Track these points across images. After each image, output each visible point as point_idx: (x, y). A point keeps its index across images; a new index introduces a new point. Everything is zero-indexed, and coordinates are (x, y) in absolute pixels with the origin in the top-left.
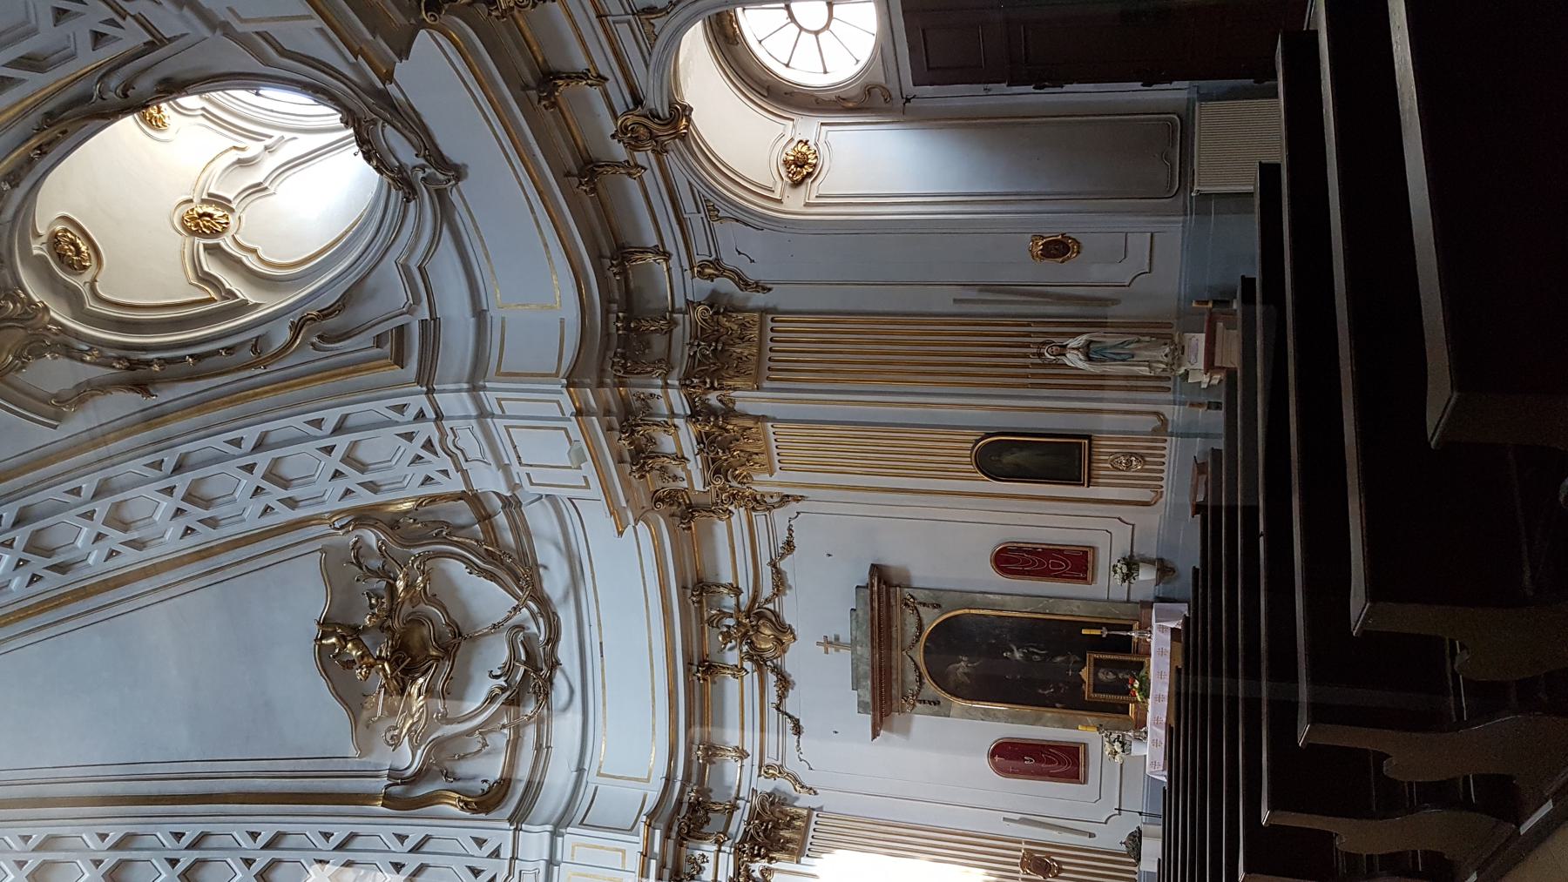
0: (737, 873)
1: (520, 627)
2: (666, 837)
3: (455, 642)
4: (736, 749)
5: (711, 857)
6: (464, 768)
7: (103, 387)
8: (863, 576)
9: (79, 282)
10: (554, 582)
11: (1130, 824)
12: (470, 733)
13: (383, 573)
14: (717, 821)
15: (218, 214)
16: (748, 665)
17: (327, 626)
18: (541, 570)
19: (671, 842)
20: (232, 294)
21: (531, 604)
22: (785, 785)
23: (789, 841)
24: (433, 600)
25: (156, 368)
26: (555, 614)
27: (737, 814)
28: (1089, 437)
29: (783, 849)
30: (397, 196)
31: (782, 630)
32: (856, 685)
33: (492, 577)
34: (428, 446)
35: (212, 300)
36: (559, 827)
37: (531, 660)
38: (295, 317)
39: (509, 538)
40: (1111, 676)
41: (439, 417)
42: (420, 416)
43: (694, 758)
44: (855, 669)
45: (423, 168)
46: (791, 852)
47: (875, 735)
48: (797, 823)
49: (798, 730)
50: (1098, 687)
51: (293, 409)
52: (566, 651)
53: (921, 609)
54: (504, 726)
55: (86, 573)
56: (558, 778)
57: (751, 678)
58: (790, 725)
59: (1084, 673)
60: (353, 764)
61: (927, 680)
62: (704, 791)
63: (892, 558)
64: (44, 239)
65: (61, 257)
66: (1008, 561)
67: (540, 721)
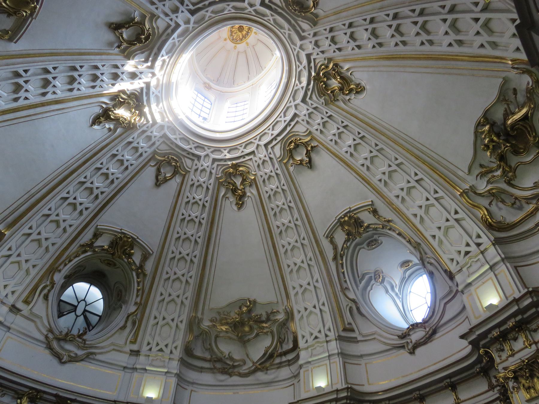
3: (243, 341)
6: (199, 343)
7: (335, 248)
9: (365, 245)
10: (261, 376)
12: (210, 344)
17: (254, 302)
18: (265, 372)
20: (360, 283)
21: (253, 368)
24: (257, 335)
25: (341, 262)
26: (249, 376)
30: (400, 333)
33: (264, 355)
34: (316, 338)
36: (179, 376)
37: (234, 367)
38: (357, 301)
39: (277, 361)
41: (327, 342)
42: (326, 336)
45: (411, 342)
51: (328, 297)
52: (235, 379)
54: (212, 356)
55: (278, 239)
56: (192, 375)
60: (206, 307)
65: (372, 241)
67: (211, 369)
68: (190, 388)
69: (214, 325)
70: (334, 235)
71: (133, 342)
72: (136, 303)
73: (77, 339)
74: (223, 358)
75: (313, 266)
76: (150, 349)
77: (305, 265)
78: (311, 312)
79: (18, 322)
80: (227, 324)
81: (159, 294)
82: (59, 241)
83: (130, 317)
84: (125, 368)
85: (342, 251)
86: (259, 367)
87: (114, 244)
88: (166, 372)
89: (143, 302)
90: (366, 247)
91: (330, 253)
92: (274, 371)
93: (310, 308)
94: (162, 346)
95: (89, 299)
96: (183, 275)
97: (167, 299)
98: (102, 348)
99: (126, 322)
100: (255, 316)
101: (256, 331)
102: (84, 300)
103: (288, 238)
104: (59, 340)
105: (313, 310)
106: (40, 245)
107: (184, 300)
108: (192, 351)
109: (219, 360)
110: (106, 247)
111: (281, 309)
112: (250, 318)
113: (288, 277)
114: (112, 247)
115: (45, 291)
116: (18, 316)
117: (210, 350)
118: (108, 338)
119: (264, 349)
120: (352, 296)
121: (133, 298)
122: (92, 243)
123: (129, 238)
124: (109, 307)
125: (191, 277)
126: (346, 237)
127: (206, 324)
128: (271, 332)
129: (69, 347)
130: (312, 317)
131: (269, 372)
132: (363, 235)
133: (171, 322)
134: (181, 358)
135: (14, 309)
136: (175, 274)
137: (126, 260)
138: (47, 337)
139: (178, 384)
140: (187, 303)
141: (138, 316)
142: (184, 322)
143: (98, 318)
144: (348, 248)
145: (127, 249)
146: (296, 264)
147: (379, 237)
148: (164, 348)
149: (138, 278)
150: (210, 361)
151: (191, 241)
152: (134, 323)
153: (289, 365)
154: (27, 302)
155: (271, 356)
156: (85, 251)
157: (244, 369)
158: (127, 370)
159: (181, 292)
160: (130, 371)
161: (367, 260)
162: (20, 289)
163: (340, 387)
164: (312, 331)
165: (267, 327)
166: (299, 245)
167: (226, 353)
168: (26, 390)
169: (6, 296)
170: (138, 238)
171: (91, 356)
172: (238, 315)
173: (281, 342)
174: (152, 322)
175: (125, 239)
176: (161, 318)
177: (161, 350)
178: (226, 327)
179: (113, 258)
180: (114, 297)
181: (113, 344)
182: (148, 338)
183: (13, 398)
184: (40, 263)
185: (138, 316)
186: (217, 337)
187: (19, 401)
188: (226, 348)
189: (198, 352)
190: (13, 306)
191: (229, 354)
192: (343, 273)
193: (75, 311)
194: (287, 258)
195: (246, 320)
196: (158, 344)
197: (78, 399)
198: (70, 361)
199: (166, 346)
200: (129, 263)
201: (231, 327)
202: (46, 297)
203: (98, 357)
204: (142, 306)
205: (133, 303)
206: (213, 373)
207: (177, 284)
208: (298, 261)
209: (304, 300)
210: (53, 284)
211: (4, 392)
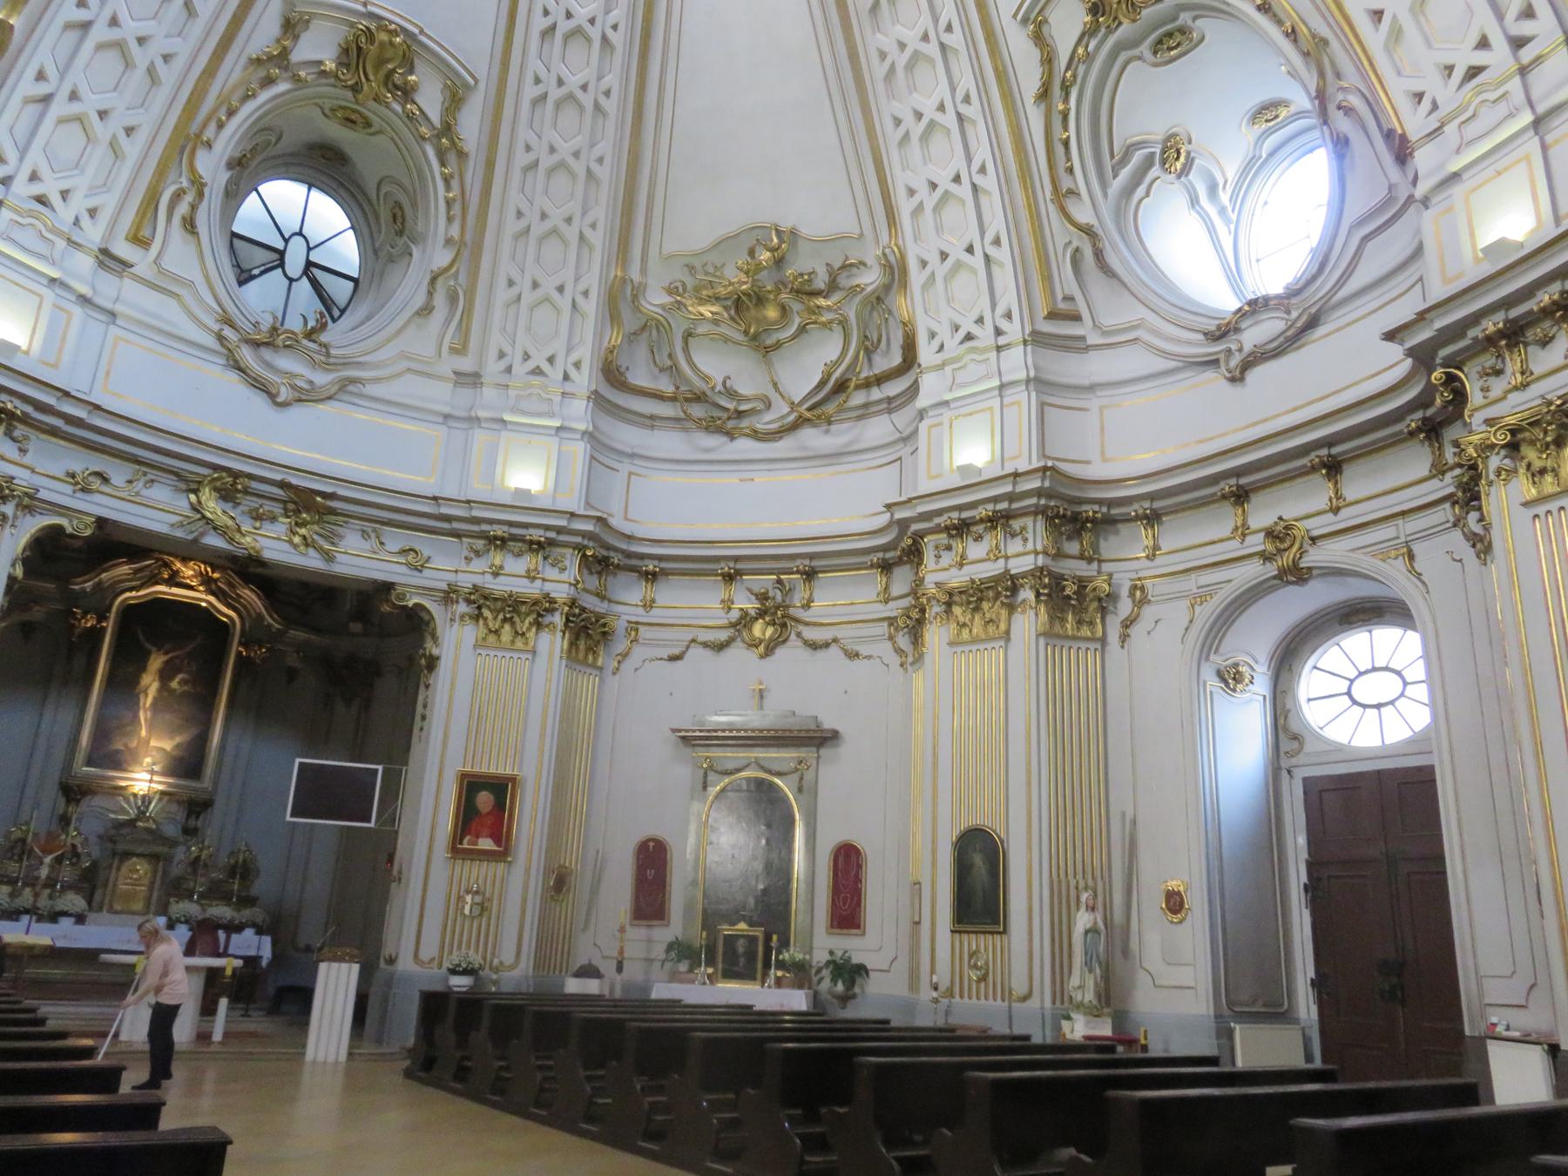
1: (769, 406)
2: (584, 534)
3: (763, 347)
6: (642, 352)
7: (1048, 60)
8: (828, 723)
9: (1145, 49)
10: (811, 437)
11: (607, 968)
12: (670, 356)
13: (833, 286)
14: (593, 582)
15: (1179, 165)
16: (735, 615)
17: (791, 236)
18: (825, 427)
19: (579, 540)
20: (1115, 177)
21: (792, 418)
22: (620, 645)
25: (1061, 107)
28: (1005, 932)
30: (1211, 326)
31: (770, 649)
33: (822, 383)
34: (969, 337)
35: (1112, 156)
36: (590, 437)
37: (740, 414)
38: (1100, 232)
40: (741, 950)
41: (999, 349)
42: (998, 332)
43: (646, 562)
45: (1240, 350)
46: (569, 651)
48: (590, 658)
49: (674, 658)
50: (730, 940)
51: (1013, 224)
52: (744, 447)
53: (796, 777)
55: (868, 31)
56: (627, 436)
58: (677, 651)
59: (742, 926)
63: (845, 750)
64: (1190, 23)
65: (1170, 35)
66: (847, 856)
68: (625, 467)
69: (679, 302)
70: (1047, 12)
71: (460, 350)
72: (449, 242)
73: (305, 342)
74: (709, 393)
75: (974, 122)
76: (509, 370)
77: (949, 119)
78: (959, 265)
79: (130, 295)
80: (717, 299)
81: (512, 213)
82: (183, 48)
83: (440, 280)
84: (447, 417)
85: (1068, 68)
86: (808, 415)
87: (354, 54)
88: (559, 429)
89: (468, 237)
90: (1148, 55)
91: (1029, 78)
92: (845, 425)
93: (958, 253)
94: (539, 360)
95: (315, 232)
96: (576, 154)
97: (538, 229)
98: (375, 366)
99: (430, 294)
100: (796, 278)
101: (797, 320)
102: (300, 234)
103: (898, 27)
104: (257, 344)
105: (966, 257)
106: (128, 64)
107: (588, 232)
108: (622, 374)
109: (699, 398)
110: (330, 65)
111: (871, 255)
112: (781, 284)
113: (893, 158)
114: (348, 66)
115: (183, 209)
116: (126, 280)
117: (673, 370)
118: (389, 340)
119: (822, 368)
120: (1083, 214)
121: (437, 225)
122: (285, 53)
123: (394, 33)
124: (376, 252)
125: (600, 160)
126: (1088, 19)
127: (656, 299)
128: (840, 322)
129: (286, 362)
130: (963, 277)
131: (833, 427)
132: (1144, 12)
133: (555, 295)
134: (596, 392)
135: (106, 257)
136: (552, 150)
137: (398, 108)
138: (220, 338)
139: (592, 457)
140: (597, 238)
141: (462, 279)
142: (594, 295)
143: (351, 285)
144: (1089, 58)
145: (394, 71)
146: (919, 116)
147: (1195, 19)
148: (546, 367)
149: (443, 164)
150: (673, 399)
151: (589, 40)
152: (453, 298)
153: (890, 411)
154: (140, 240)
155: (841, 387)
156: (269, 81)
157: (766, 421)
158: (451, 423)
159: (574, 207)
160: (465, 425)
161: (1147, 102)
162: (108, 202)
163: (1023, 467)
164: (958, 320)
165: (829, 308)
166: (932, 49)
167: (718, 378)
168: (205, 471)
169: (77, 222)
170: (422, 31)
171: (351, 388)
172: (747, 273)
173: (869, 349)
174: (502, 295)
175: (384, 37)
176: (528, 284)
177: (538, 371)
178: (714, 309)
179: (357, 102)
180: (385, 220)
181: (403, 356)
182: (496, 340)
183: (177, 490)
184: (144, 122)
185: (462, 279)
186: (688, 335)
187: (193, 497)
188: (721, 365)
189: (640, 376)
190: (105, 252)
191: (724, 383)
192: (1066, 143)
193: (281, 264)
194: (891, 95)
195: (768, 291)
196: (527, 357)
197: (341, 492)
198: (300, 400)
199: (551, 360)
200: (410, 117)
201: (726, 308)
202: (190, 225)
203: (370, 389)
204: (469, 249)
205: (441, 241)
206: (686, 430)
207: (561, 181)
208: (929, 107)
209: (939, 230)
210: (199, 186)
211: (150, 477)
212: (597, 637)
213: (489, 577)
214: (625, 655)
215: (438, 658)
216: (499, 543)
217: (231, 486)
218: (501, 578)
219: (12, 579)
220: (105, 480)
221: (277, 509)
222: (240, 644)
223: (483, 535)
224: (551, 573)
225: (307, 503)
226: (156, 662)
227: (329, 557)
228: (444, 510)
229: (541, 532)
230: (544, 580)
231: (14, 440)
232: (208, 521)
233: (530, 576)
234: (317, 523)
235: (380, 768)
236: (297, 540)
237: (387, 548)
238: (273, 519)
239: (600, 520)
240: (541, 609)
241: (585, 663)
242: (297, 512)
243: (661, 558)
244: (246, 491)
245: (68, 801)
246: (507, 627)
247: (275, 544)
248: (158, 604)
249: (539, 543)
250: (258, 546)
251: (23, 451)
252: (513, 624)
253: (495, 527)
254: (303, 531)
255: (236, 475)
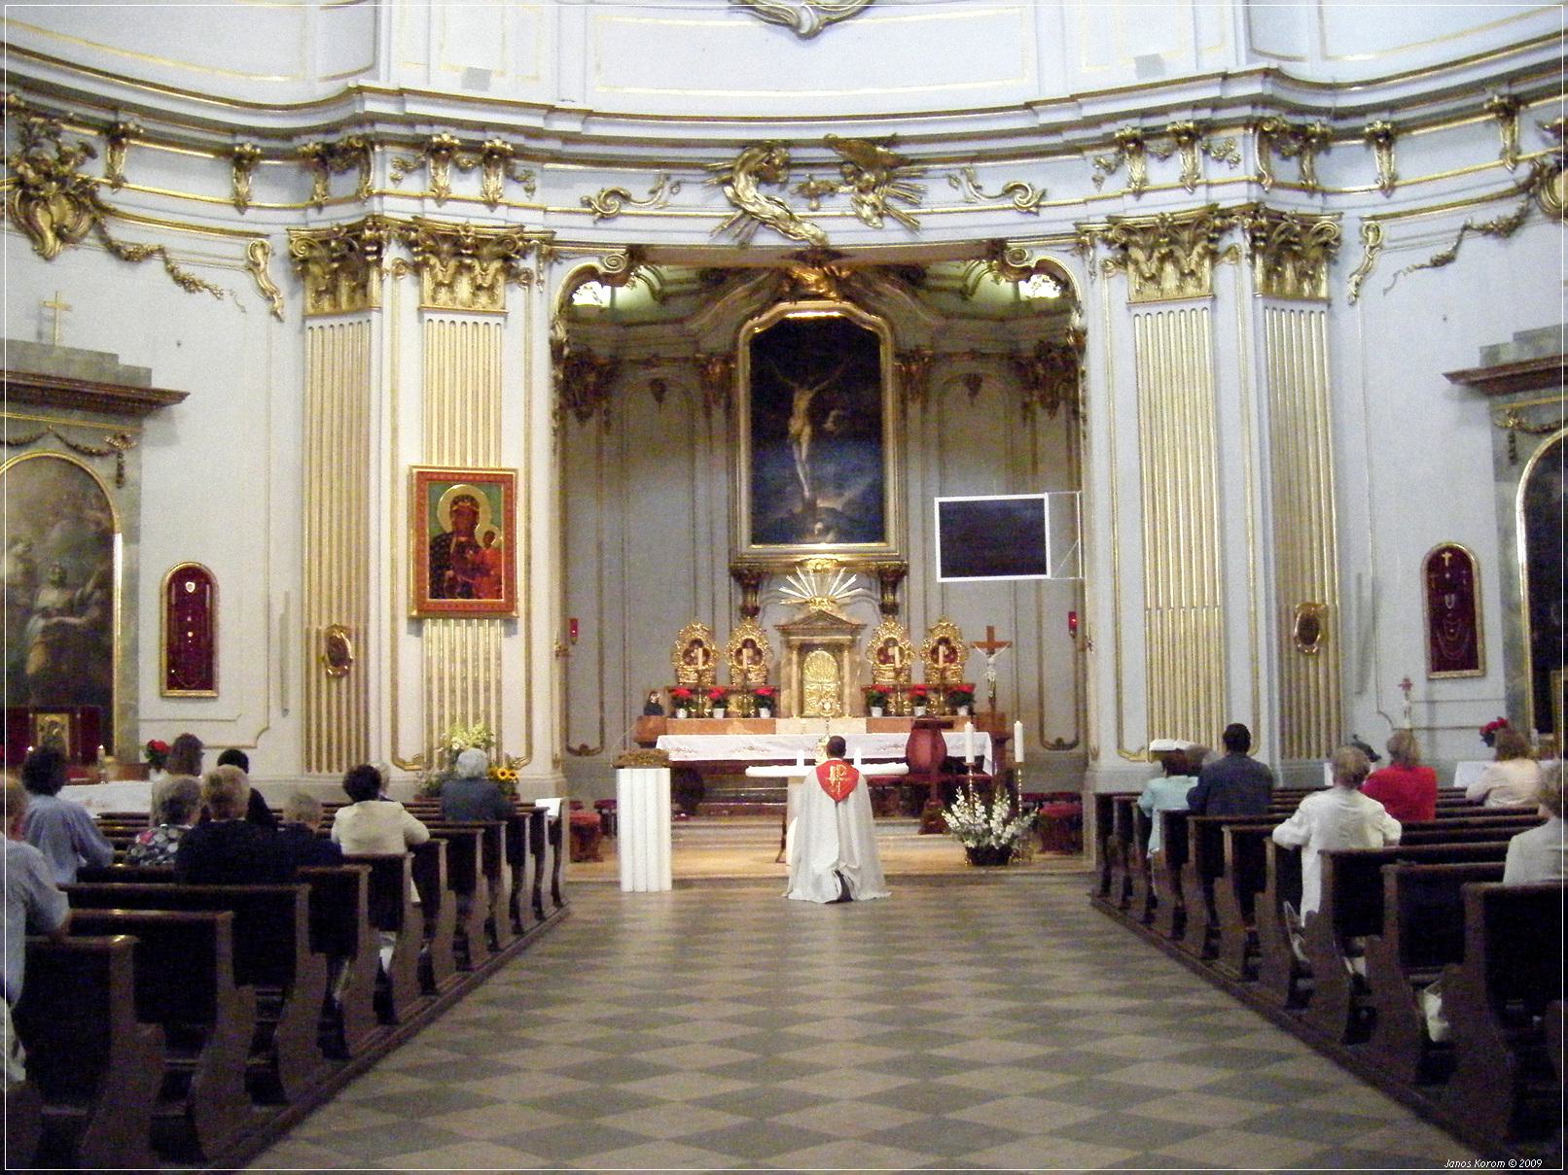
0: (1225, 214)
2: (1254, 101)
4: (1394, 178)
5: (1239, 173)
16: (1524, 171)
19: (1246, 111)
22: (1353, 257)
23: (1281, 276)
27: (1302, 197)
29: (1269, 273)
32: (1523, 338)
43: (1370, 118)
44: (1543, 333)
47: (1454, 377)
48: (1306, 286)
57: (1506, 179)
58: (1443, 250)
61: (1548, 441)
62: (1325, 141)
168: (733, 153)
187: (729, 190)
197: (903, 132)
198: (830, 23)
211: (675, 179)
212: (1315, 253)
213: (1130, 200)
214: (1365, 272)
215: (1085, 333)
216: (1136, 145)
217: (769, 162)
218: (1146, 197)
219: (556, 349)
220: (626, 198)
221: (833, 177)
222: (898, 355)
223: (1108, 141)
224: (1216, 172)
225: (874, 161)
226: (802, 401)
227: (912, 225)
228: (1047, 118)
229: (1187, 114)
230: (1209, 185)
231: (516, 180)
232: (750, 216)
233: (1190, 182)
234: (888, 181)
235: (1045, 496)
236: (867, 211)
237: (986, 192)
238: (832, 191)
239: (1267, 73)
240: (1206, 229)
241: (1297, 296)
242: (858, 174)
243: (1391, 107)
244: (788, 164)
245: (745, 593)
246: (1169, 268)
247: (843, 222)
248: (786, 328)
249: (1187, 132)
250: (820, 233)
251: (530, 190)
252: (1176, 262)
253: (1121, 124)
254: (871, 198)
255: (769, 147)
